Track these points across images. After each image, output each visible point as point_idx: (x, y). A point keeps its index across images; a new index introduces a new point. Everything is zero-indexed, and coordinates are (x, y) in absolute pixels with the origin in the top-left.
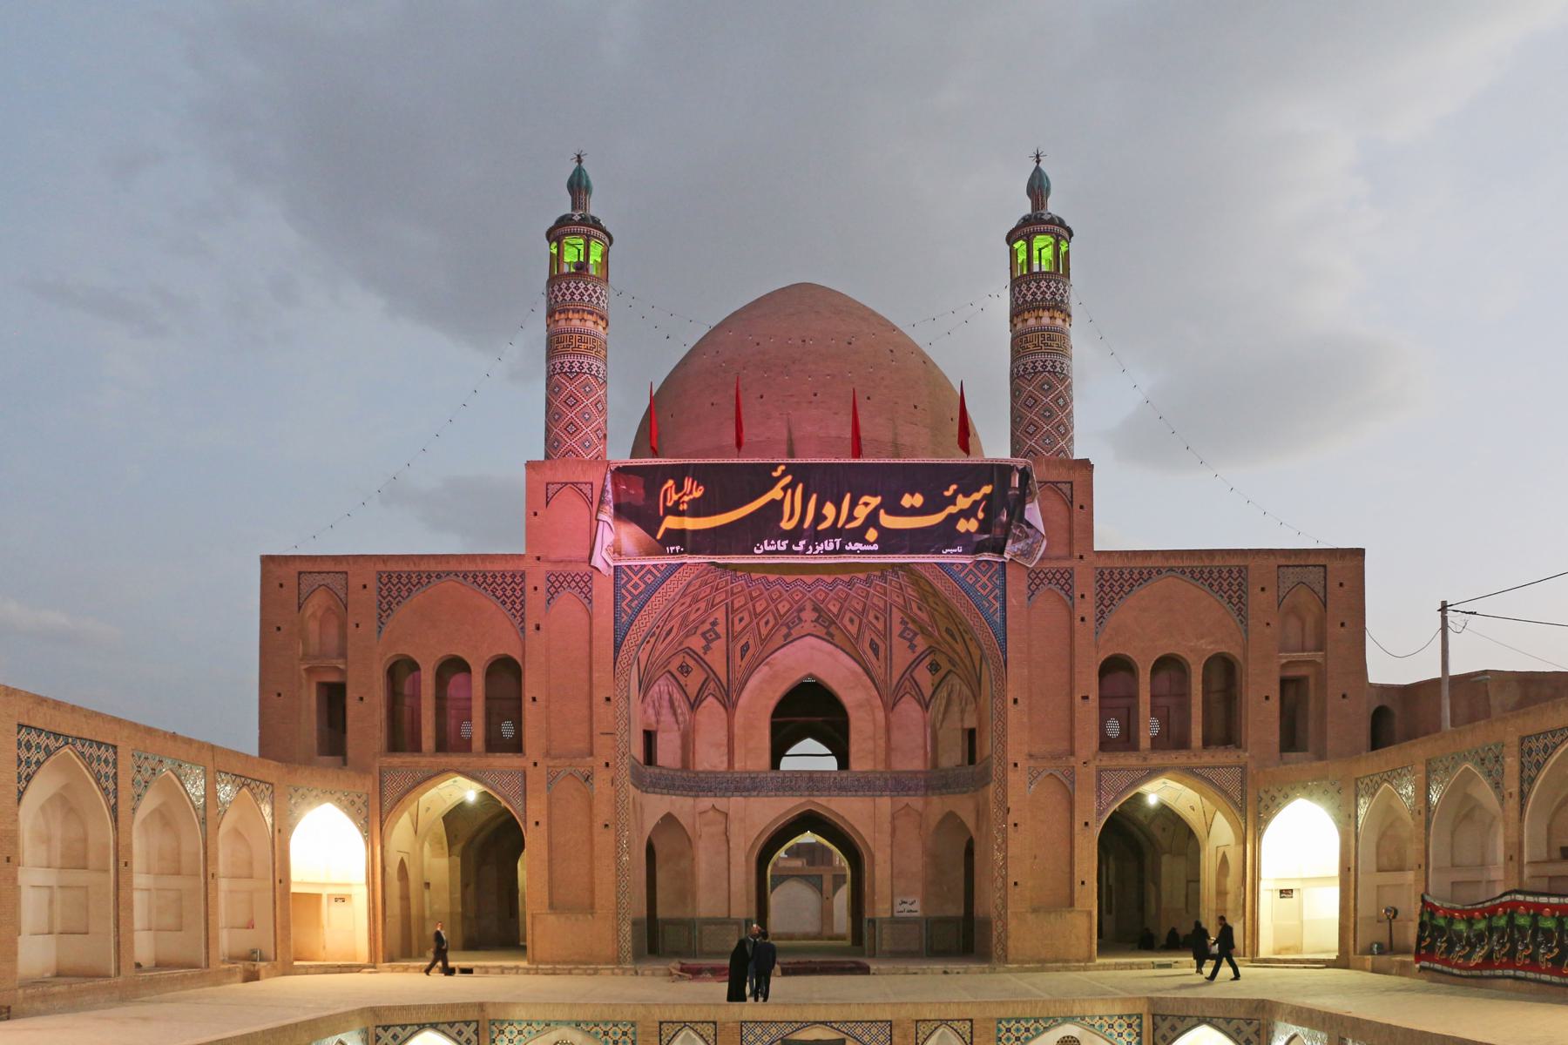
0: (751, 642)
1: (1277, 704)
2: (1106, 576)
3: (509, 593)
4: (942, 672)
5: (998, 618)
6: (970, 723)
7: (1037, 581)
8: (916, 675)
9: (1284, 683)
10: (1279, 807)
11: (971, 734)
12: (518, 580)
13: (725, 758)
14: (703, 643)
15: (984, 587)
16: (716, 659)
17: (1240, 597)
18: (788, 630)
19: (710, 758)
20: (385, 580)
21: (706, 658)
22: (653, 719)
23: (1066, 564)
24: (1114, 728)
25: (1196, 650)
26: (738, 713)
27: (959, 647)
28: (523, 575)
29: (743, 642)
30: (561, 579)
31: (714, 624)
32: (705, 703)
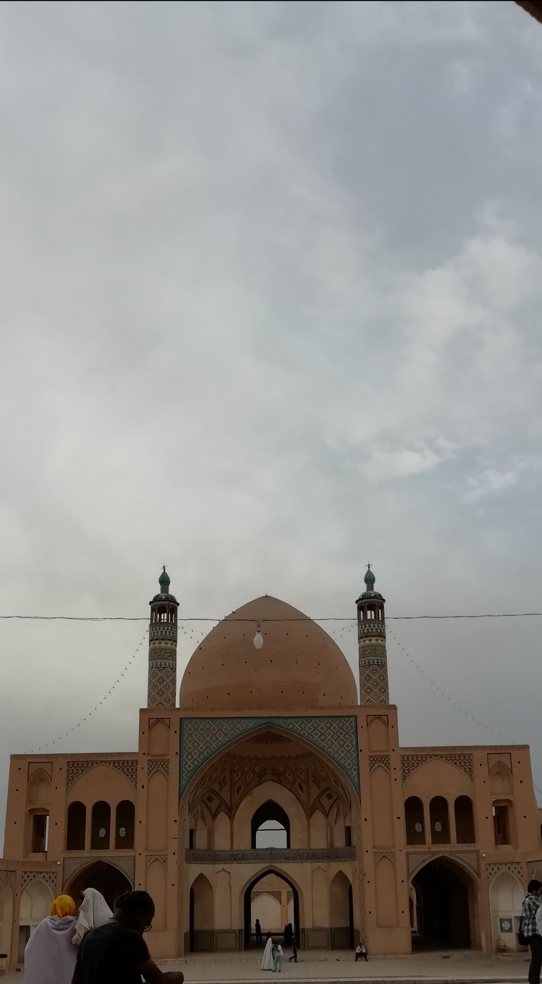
0: (242, 786)
2: (406, 759)
3: (130, 771)
5: (356, 779)
6: (348, 825)
7: (374, 762)
8: (321, 800)
11: (348, 830)
14: (219, 786)
15: (349, 765)
17: (470, 769)
19: (222, 843)
21: (220, 794)
26: (236, 819)
27: (340, 789)
28: (137, 762)
29: (238, 785)
30: (155, 763)
31: (225, 778)
32: (219, 815)
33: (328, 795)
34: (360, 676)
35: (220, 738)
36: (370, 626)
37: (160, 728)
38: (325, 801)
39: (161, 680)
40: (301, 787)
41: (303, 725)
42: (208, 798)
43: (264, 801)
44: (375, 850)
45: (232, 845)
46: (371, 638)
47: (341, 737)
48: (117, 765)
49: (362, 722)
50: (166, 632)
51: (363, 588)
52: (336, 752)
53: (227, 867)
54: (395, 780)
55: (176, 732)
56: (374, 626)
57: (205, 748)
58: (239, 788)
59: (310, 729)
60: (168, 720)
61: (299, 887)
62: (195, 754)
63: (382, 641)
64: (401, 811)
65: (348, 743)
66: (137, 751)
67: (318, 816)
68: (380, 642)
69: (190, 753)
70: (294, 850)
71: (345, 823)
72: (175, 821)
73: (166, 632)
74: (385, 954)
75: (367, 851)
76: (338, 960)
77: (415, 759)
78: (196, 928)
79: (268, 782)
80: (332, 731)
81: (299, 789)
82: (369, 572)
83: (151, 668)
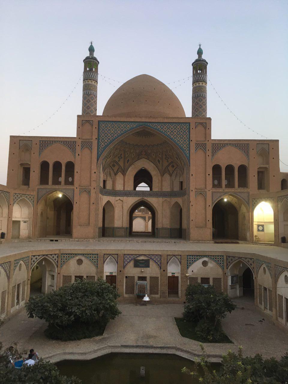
1: (257, 178)
3: (72, 146)
4: (175, 168)
6: (181, 180)
7: (198, 146)
9: (258, 172)
10: (258, 203)
11: (181, 183)
12: (74, 143)
13: (123, 187)
16: (121, 164)
18: (139, 157)
19: (119, 187)
20: (41, 142)
22: (106, 178)
23: (205, 142)
24: (216, 182)
25: (236, 163)
26: (126, 177)
28: (75, 143)
29: (128, 159)
31: (121, 155)
32: (118, 174)
33: (172, 166)
34: (192, 103)
35: (119, 132)
36: (199, 76)
37: (87, 126)
38: (170, 168)
39: (89, 101)
40: (159, 161)
41: (162, 127)
42: (113, 165)
43: (140, 168)
44: (196, 190)
45: (124, 188)
46: (200, 83)
47: (182, 133)
48: (65, 143)
49: (192, 126)
50: (91, 76)
51: (196, 57)
52: (178, 141)
53: (121, 198)
54: (208, 156)
55: (96, 128)
56: (202, 76)
57: (111, 136)
58: (128, 161)
59: (165, 129)
60: (92, 121)
61: (155, 208)
62: (106, 139)
63: (205, 84)
64: (210, 171)
65: (185, 136)
66: (76, 137)
67: (167, 176)
68: (204, 85)
69: (102, 139)
70: (154, 191)
71: (179, 179)
72: (95, 172)
73: (91, 76)
74: (200, 240)
75: (192, 190)
76: (175, 242)
77: (219, 146)
78: (106, 226)
79: (143, 159)
80: (177, 130)
81: (157, 162)
82: (200, 48)
83: (84, 95)
